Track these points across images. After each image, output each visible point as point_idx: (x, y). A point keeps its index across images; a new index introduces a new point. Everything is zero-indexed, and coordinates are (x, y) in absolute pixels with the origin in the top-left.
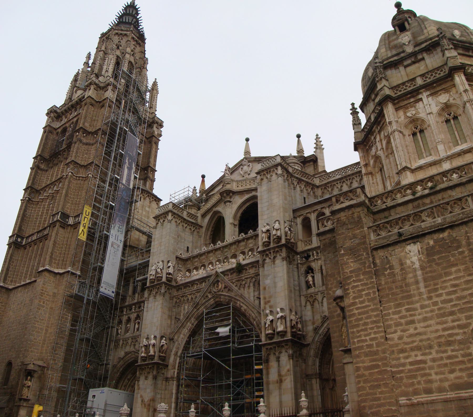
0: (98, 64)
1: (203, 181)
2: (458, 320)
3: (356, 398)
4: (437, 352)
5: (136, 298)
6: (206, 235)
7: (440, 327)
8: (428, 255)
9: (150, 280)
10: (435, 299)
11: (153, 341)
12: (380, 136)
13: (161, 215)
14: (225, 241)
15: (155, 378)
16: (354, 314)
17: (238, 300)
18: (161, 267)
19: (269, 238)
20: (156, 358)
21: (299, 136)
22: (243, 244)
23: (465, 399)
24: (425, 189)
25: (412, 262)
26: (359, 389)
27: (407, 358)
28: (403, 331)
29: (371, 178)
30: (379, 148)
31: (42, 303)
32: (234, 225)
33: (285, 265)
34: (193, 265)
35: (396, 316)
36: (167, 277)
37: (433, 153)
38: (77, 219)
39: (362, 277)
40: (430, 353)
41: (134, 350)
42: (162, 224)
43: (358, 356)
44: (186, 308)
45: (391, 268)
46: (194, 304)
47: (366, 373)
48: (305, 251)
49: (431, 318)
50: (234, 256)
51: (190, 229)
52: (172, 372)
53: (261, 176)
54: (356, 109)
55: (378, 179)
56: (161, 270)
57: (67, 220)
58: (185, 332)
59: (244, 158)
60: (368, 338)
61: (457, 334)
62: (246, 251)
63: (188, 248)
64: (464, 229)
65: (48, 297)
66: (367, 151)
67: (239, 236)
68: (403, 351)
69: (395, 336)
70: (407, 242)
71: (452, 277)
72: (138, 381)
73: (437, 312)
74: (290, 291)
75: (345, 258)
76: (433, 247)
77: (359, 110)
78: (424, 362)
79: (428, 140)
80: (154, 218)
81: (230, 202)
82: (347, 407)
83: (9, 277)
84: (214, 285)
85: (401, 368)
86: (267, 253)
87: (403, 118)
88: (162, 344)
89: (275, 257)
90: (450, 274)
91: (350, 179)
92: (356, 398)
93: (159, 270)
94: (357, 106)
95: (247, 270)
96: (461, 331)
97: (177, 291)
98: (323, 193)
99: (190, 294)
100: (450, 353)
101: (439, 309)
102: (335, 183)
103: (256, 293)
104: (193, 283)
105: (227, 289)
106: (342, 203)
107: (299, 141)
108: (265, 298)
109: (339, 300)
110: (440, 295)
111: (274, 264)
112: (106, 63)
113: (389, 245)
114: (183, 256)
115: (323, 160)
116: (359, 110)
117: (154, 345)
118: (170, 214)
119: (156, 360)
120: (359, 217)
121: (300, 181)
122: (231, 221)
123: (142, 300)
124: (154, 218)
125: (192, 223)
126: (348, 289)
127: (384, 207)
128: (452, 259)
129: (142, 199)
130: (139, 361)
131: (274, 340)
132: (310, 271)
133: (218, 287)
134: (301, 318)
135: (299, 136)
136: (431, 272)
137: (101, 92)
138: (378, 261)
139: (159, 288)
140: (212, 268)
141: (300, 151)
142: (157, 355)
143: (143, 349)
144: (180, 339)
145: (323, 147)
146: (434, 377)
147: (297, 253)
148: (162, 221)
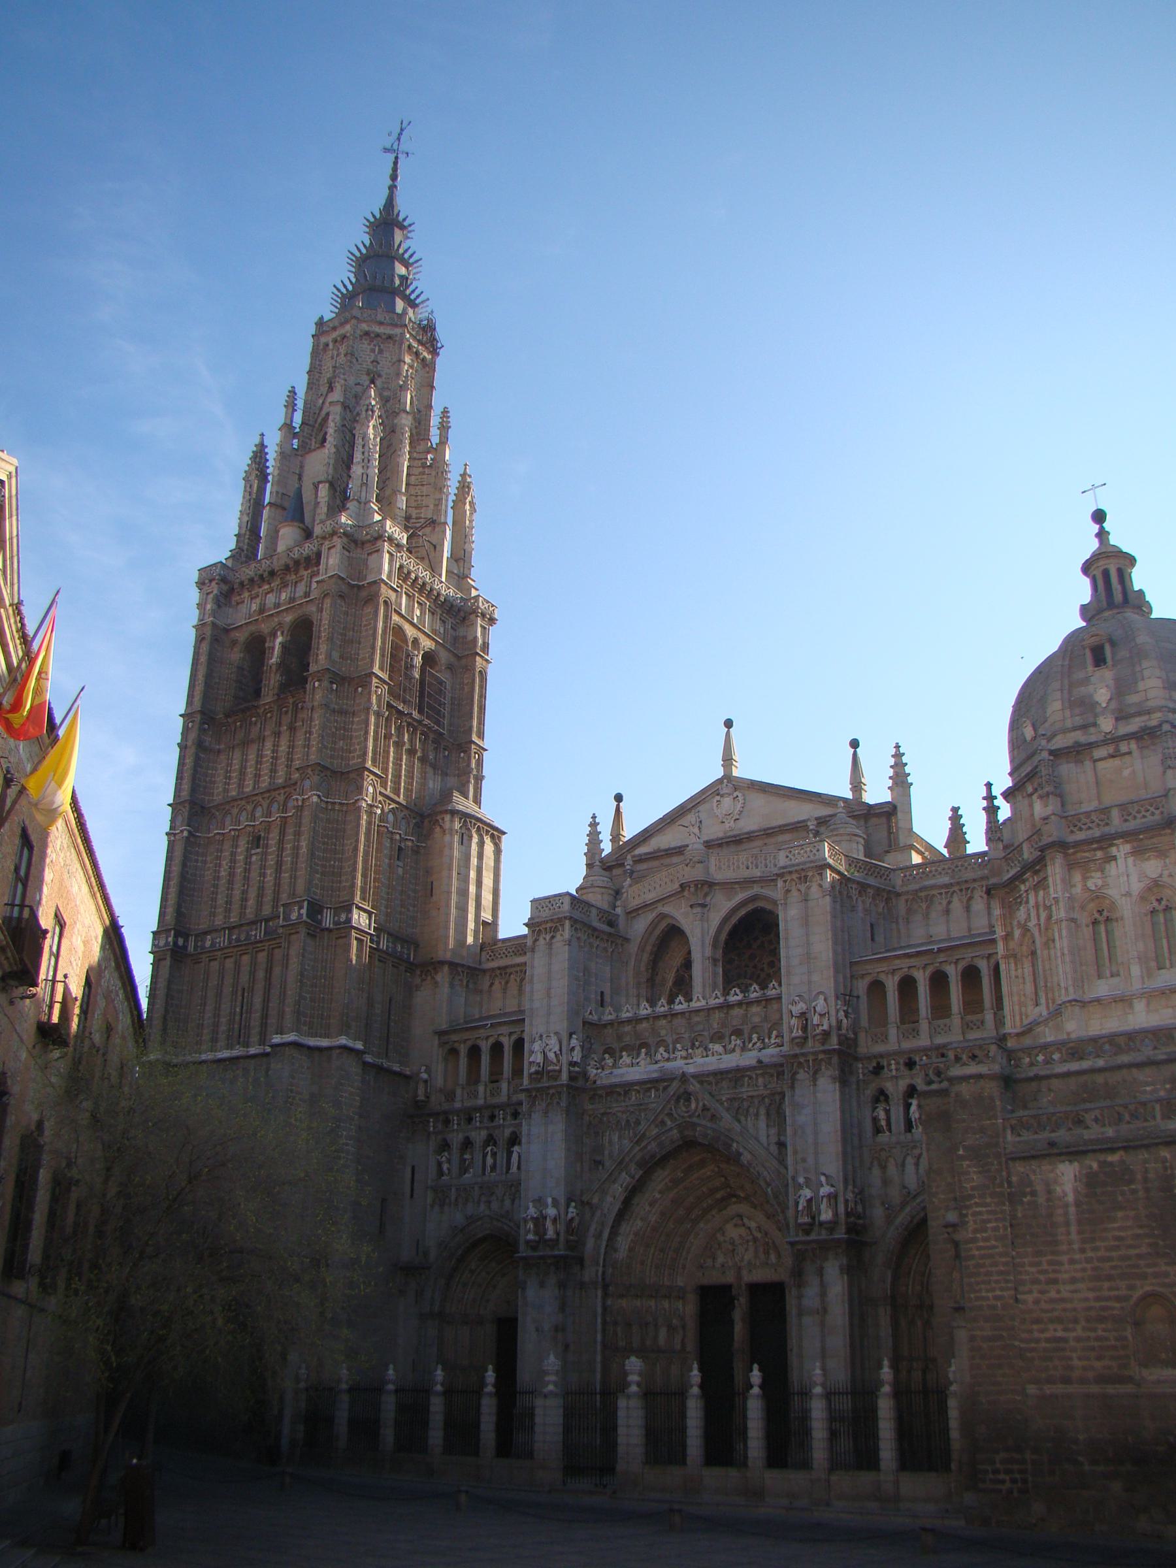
1: (618, 812)
2: (1118, 1289)
4: (1084, 1329)
7: (1091, 1295)
9: (531, 1075)
10: (1090, 1254)
11: (551, 1212)
12: (1036, 896)
14: (695, 999)
15: (562, 1285)
16: (973, 1256)
17: (733, 1140)
18: (557, 1049)
19: (805, 1028)
20: (561, 1245)
21: (855, 744)
22: (736, 1012)
24: (1098, 1056)
25: (1063, 1191)
27: (1042, 1331)
28: (1042, 1292)
29: (1012, 966)
30: (1034, 921)
32: (715, 961)
33: (838, 1093)
34: (620, 1038)
35: (1033, 1269)
36: (570, 1072)
37: (1122, 973)
38: (343, 917)
39: (988, 1200)
40: (1074, 1330)
41: (487, 1212)
42: (550, 945)
44: (617, 1143)
45: (1033, 1193)
46: (635, 1135)
48: (875, 1057)
50: (718, 1037)
51: (605, 949)
53: (785, 881)
54: (995, 798)
55: (1026, 971)
56: (556, 1055)
58: (618, 1190)
59: (728, 777)
60: (990, 1295)
62: (746, 1029)
63: (602, 993)
66: (1010, 907)
67: (726, 993)
68: (1037, 1321)
69: (1030, 1298)
70: (1063, 1158)
71: (1116, 1225)
72: (524, 1289)
73: (1089, 1272)
74: (845, 1141)
75: (966, 1163)
77: (1000, 802)
78: (1064, 1340)
79: (1117, 943)
81: (703, 906)
82: (953, 1388)
85: (1033, 1345)
86: (802, 1060)
88: (570, 1216)
89: (815, 1073)
91: (967, 889)
93: (551, 1056)
94: (997, 791)
95: (750, 1078)
96: (1117, 1305)
98: (909, 911)
99: (623, 1112)
100: (1100, 1333)
101: (1094, 1269)
102: (935, 892)
103: (773, 1131)
104: (627, 1088)
106: (965, 1064)
107: (855, 755)
108: (795, 1152)
109: (950, 1230)
111: (815, 1085)
113: (1033, 1157)
114: (596, 1018)
117: (555, 1221)
119: (561, 1251)
122: (708, 952)
123: (495, 1101)
126: (966, 1215)
127: (1031, 1074)
128: (1120, 1198)
130: (522, 1247)
131: (813, 1236)
132: (882, 1098)
134: (861, 1192)
135: (855, 744)
138: (1014, 1179)
141: (857, 785)
142: (562, 1238)
143: (531, 1225)
145: (910, 779)
146: (1076, 1362)
147: (857, 1059)
148: (548, 937)
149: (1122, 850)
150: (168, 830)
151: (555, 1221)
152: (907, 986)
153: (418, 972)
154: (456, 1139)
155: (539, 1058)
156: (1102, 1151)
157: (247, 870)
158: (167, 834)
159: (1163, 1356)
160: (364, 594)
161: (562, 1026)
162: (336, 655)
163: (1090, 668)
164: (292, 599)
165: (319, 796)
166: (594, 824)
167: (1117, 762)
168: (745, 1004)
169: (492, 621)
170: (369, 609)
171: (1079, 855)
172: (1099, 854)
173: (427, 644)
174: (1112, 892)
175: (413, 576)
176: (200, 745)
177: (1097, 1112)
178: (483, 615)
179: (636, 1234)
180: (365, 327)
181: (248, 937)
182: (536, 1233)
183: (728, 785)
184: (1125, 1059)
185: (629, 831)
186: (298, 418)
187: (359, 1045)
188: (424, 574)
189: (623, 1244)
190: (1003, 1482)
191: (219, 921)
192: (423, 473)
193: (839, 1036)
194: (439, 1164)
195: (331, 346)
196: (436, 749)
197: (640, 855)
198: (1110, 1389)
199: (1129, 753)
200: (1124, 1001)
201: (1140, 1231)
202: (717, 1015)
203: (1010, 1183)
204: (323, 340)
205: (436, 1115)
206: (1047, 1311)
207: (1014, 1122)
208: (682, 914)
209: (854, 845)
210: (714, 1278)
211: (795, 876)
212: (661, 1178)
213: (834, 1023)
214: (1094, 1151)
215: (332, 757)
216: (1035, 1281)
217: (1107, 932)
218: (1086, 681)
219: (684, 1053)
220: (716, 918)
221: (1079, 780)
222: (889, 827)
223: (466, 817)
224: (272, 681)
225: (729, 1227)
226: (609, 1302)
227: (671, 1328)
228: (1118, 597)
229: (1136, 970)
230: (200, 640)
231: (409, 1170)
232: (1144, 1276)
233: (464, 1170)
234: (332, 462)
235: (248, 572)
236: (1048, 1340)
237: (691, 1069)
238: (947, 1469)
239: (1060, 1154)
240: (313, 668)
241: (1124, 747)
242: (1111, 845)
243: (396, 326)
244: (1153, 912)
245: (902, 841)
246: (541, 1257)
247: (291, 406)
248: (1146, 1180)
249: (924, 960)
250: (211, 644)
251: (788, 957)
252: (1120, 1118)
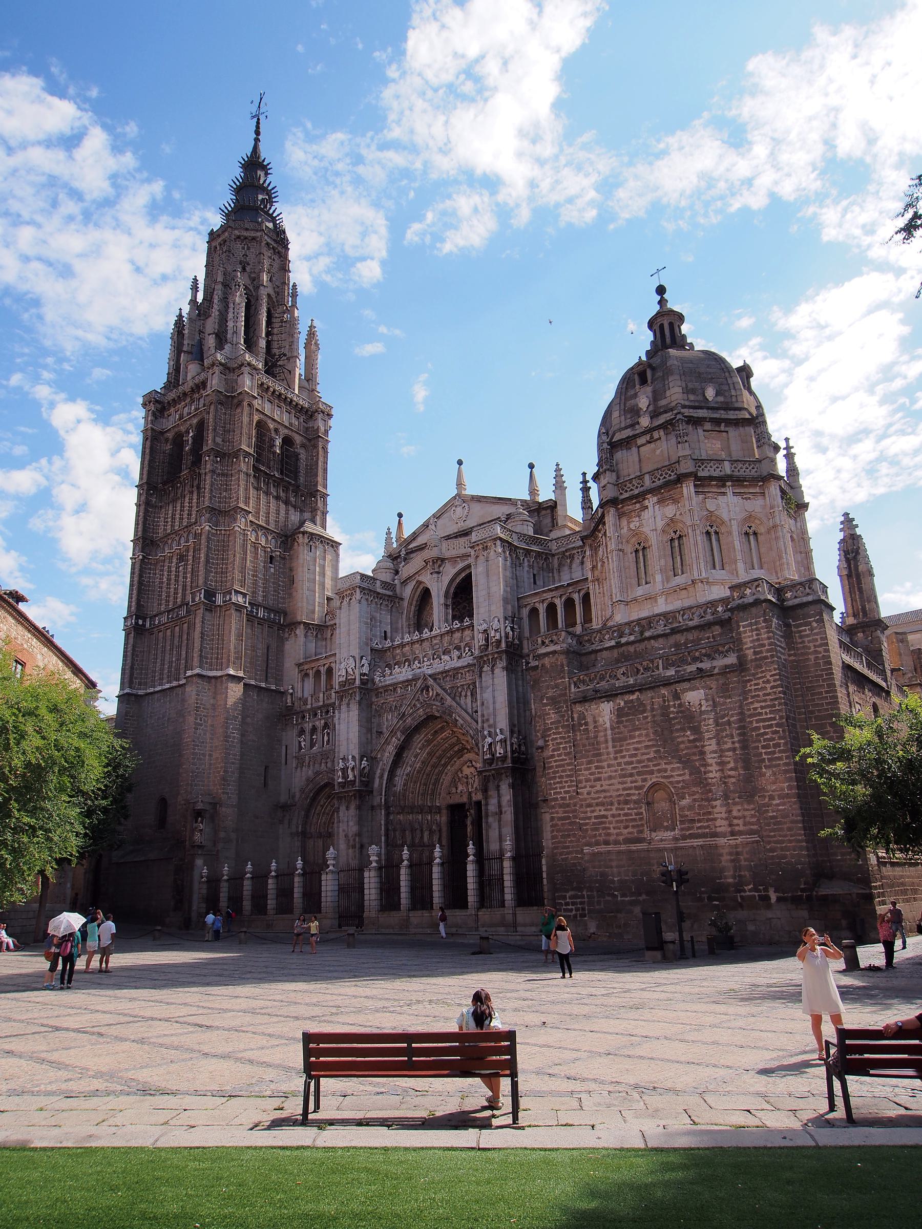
3: (550, 846)
4: (617, 809)
5: (321, 699)
6: (409, 612)
7: (621, 786)
8: (618, 716)
11: (351, 763)
15: (359, 808)
19: (487, 640)
20: (357, 784)
21: (531, 466)
22: (457, 635)
23: (634, 851)
24: (631, 634)
26: (553, 837)
27: (593, 812)
28: (592, 787)
31: (198, 721)
32: (446, 606)
34: (394, 658)
35: (587, 772)
39: (561, 730)
40: (611, 809)
42: (349, 603)
43: (553, 807)
45: (586, 724)
47: (560, 823)
49: (614, 778)
52: (379, 799)
61: (634, 794)
62: (462, 645)
63: (385, 632)
64: (650, 694)
68: (589, 805)
69: (585, 791)
72: (338, 812)
76: (623, 708)
77: (591, 484)
78: (605, 817)
81: (438, 573)
83: (136, 678)
84: (422, 691)
87: (626, 529)
89: (493, 666)
90: (634, 737)
92: (550, 846)
93: (350, 670)
100: (626, 811)
101: (622, 770)
104: (395, 686)
105: (439, 698)
108: (483, 715)
110: (624, 757)
115: (565, 505)
116: (591, 484)
117: (353, 769)
120: (562, 665)
121: (528, 552)
122: (442, 601)
125: (389, 596)
128: (637, 723)
130: (336, 787)
133: (428, 694)
134: (525, 738)
135: (531, 466)
136: (619, 733)
138: (575, 716)
140: (418, 665)
141: (533, 491)
144: (385, 758)
145: (565, 485)
146: (612, 831)
149: (651, 501)
151: (353, 769)
152: (551, 608)
154: (308, 727)
156: (625, 693)
157: (177, 576)
159: (665, 824)
160: (235, 401)
161: (356, 652)
162: (219, 440)
163: (638, 387)
164: (196, 409)
166: (389, 533)
167: (653, 445)
168: (462, 629)
169: (330, 416)
170: (239, 410)
171: (625, 508)
172: (638, 506)
173: (283, 432)
174: (646, 530)
176: (148, 503)
177: (624, 669)
179: (407, 775)
180: (237, 233)
182: (343, 778)
183: (461, 499)
184: (647, 634)
185: (407, 533)
186: (200, 297)
187: (241, 674)
188: (279, 388)
189: (399, 781)
190: (571, 910)
192: (281, 326)
193: (507, 642)
194: (300, 742)
196: (295, 496)
198: (633, 847)
199: (660, 438)
200: (651, 598)
201: (650, 743)
202: (446, 639)
203: (573, 718)
204: (213, 244)
205: (297, 713)
206: (594, 799)
207: (575, 679)
208: (428, 579)
209: (525, 527)
210: (457, 800)
211: (481, 547)
212: (419, 740)
213: (503, 635)
214: (621, 694)
215: (220, 502)
216: (587, 780)
217: (644, 555)
218: (635, 396)
219: (428, 663)
220: (446, 580)
221: (628, 460)
222: (553, 516)
224: (187, 460)
225: (465, 768)
226: (391, 818)
227: (431, 832)
228: (668, 340)
229: (658, 578)
230: (145, 439)
231: (284, 748)
232: (652, 772)
233: (312, 745)
234: (217, 321)
235: (172, 395)
236: (596, 817)
237: (430, 672)
238: (543, 905)
239: (601, 698)
240: (205, 449)
241: (656, 435)
242: (644, 499)
243: (257, 231)
244: (672, 540)
245: (560, 522)
246: (345, 792)
247: (195, 288)
248: (653, 710)
249: (560, 592)
250: (151, 441)
251: (477, 597)
252: (638, 671)
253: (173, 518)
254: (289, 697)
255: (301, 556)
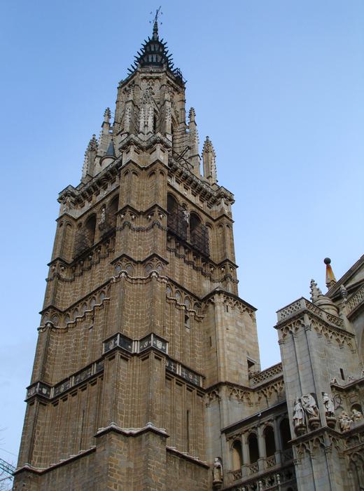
0: (128, 120)
1: (329, 268)
13: (290, 320)
18: (313, 403)
36: (328, 421)
38: (146, 344)
51: (338, 340)
56: (315, 409)
57: (130, 347)
63: (341, 370)
65: (121, 476)
80: (276, 327)
83: (36, 453)
97: (348, 442)
112: (142, 115)
118: (306, 317)
123: (272, 469)
124: (276, 327)
129: (229, 308)
137: (145, 154)
139: (317, 440)
150: (39, 326)
153: (207, 395)
155: (299, 415)
158: (38, 329)
160: (149, 171)
165: (126, 273)
170: (153, 177)
175: (179, 171)
178: (225, 196)
180: (144, 75)
181: (87, 376)
185: (338, 276)
186: (112, 121)
191: (68, 376)
195: (128, 88)
197: (350, 287)
223: (227, 295)
253: (83, 286)
254: (216, 471)
255: (219, 316)
